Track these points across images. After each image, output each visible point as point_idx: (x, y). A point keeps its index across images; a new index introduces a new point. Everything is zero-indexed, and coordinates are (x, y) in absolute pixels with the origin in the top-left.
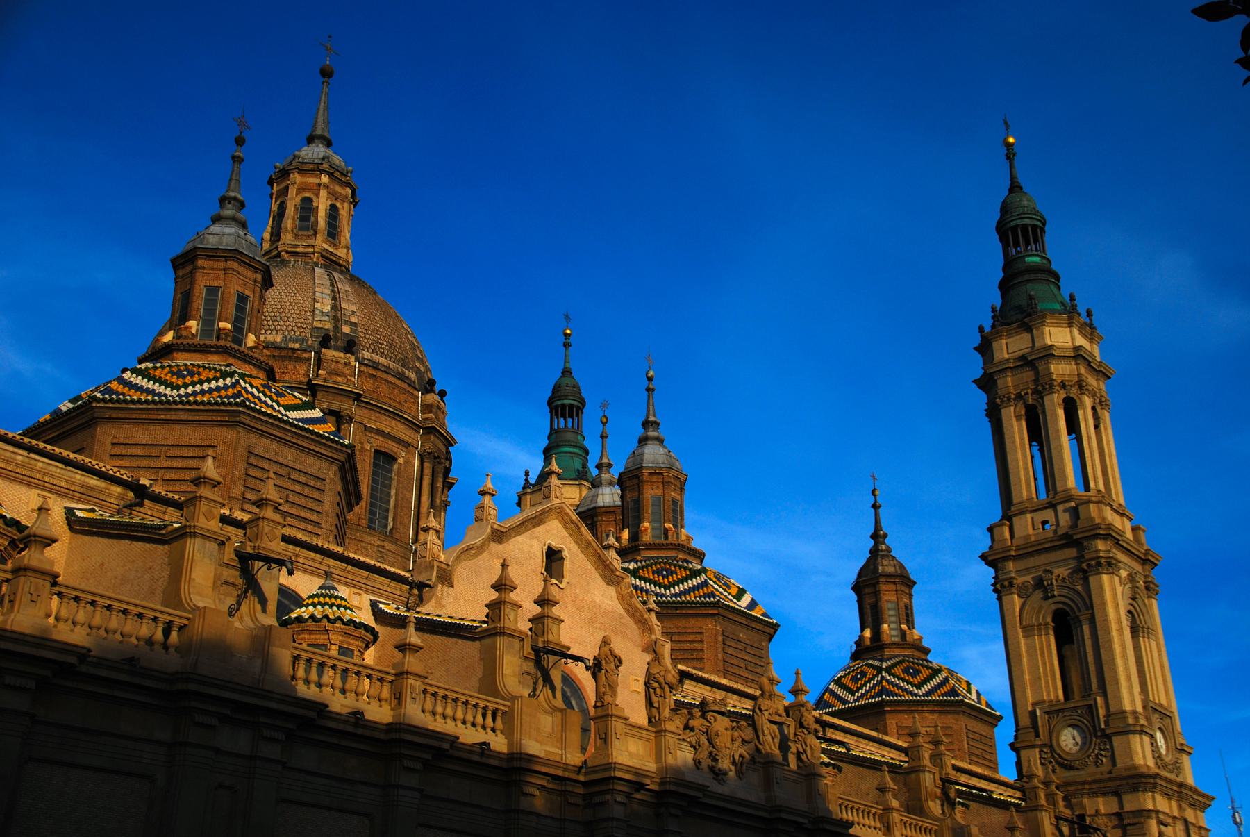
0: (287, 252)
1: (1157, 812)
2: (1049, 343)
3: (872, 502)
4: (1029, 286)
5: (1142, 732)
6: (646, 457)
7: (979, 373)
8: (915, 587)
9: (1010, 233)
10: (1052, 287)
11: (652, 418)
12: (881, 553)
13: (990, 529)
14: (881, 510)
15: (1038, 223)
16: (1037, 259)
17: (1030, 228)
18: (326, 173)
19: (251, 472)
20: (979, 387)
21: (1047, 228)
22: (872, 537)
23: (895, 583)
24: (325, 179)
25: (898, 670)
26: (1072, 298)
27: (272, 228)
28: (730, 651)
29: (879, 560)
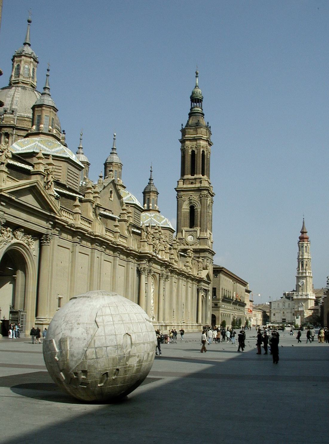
0: (22, 82)
3: (150, 170)
6: (114, 159)
8: (159, 194)
9: (194, 100)
11: (115, 148)
12: (151, 184)
13: (178, 182)
14: (152, 172)
16: (200, 109)
17: (200, 100)
18: (33, 58)
19: (69, 174)
20: (180, 142)
21: (203, 100)
22: (149, 179)
24: (32, 60)
26: (208, 123)
27: (15, 72)
28: (135, 215)
29: (151, 186)
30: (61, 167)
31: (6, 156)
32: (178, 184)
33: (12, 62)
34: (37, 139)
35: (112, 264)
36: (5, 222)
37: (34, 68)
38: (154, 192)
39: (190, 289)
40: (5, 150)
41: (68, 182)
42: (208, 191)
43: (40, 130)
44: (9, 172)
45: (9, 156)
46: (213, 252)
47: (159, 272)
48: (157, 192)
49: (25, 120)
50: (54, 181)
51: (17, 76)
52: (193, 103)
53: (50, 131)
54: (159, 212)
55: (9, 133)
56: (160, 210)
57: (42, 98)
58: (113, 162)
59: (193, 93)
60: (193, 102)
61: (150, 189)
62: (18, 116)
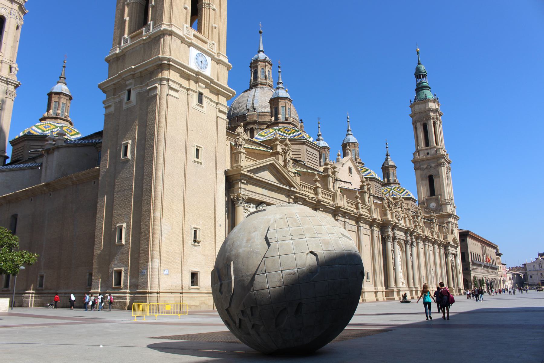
0: (260, 84)
1: (451, 222)
2: (430, 107)
4: (424, 90)
5: (449, 204)
7: (410, 113)
9: (419, 76)
10: (429, 91)
11: (350, 129)
13: (413, 154)
15: (426, 74)
16: (426, 83)
19: (308, 155)
23: (393, 168)
24: (267, 64)
25: (395, 189)
28: (376, 189)
30: (300, 149)
31: (243, 138)
32: (414, 156)
33: (250, 69)
34: (275, 128)
35: (356, 234)
36: (247, 198)
37: (269, 70)
38: (392, 166)
39: (437, 254)
40: (241, 133)
41: (308, 163)
42: (444, 159)
43: (279, 120)
44: (246, 153)
45: (245, 138)
46: (457, 216)
47: (404, 238)
48: (395, 166)
49: (266, 115)
50: (291, 159)
51: (255, 79)
52: (418, 79)
53: (286, 119)
54: (399, 184)
55: (253, 128)
56: (399, 183)
57: (277, 91)
58: (350, 142)
59: (418, 69)
60: (418, 78)
61: (388, 164)
62: (260, 112)
